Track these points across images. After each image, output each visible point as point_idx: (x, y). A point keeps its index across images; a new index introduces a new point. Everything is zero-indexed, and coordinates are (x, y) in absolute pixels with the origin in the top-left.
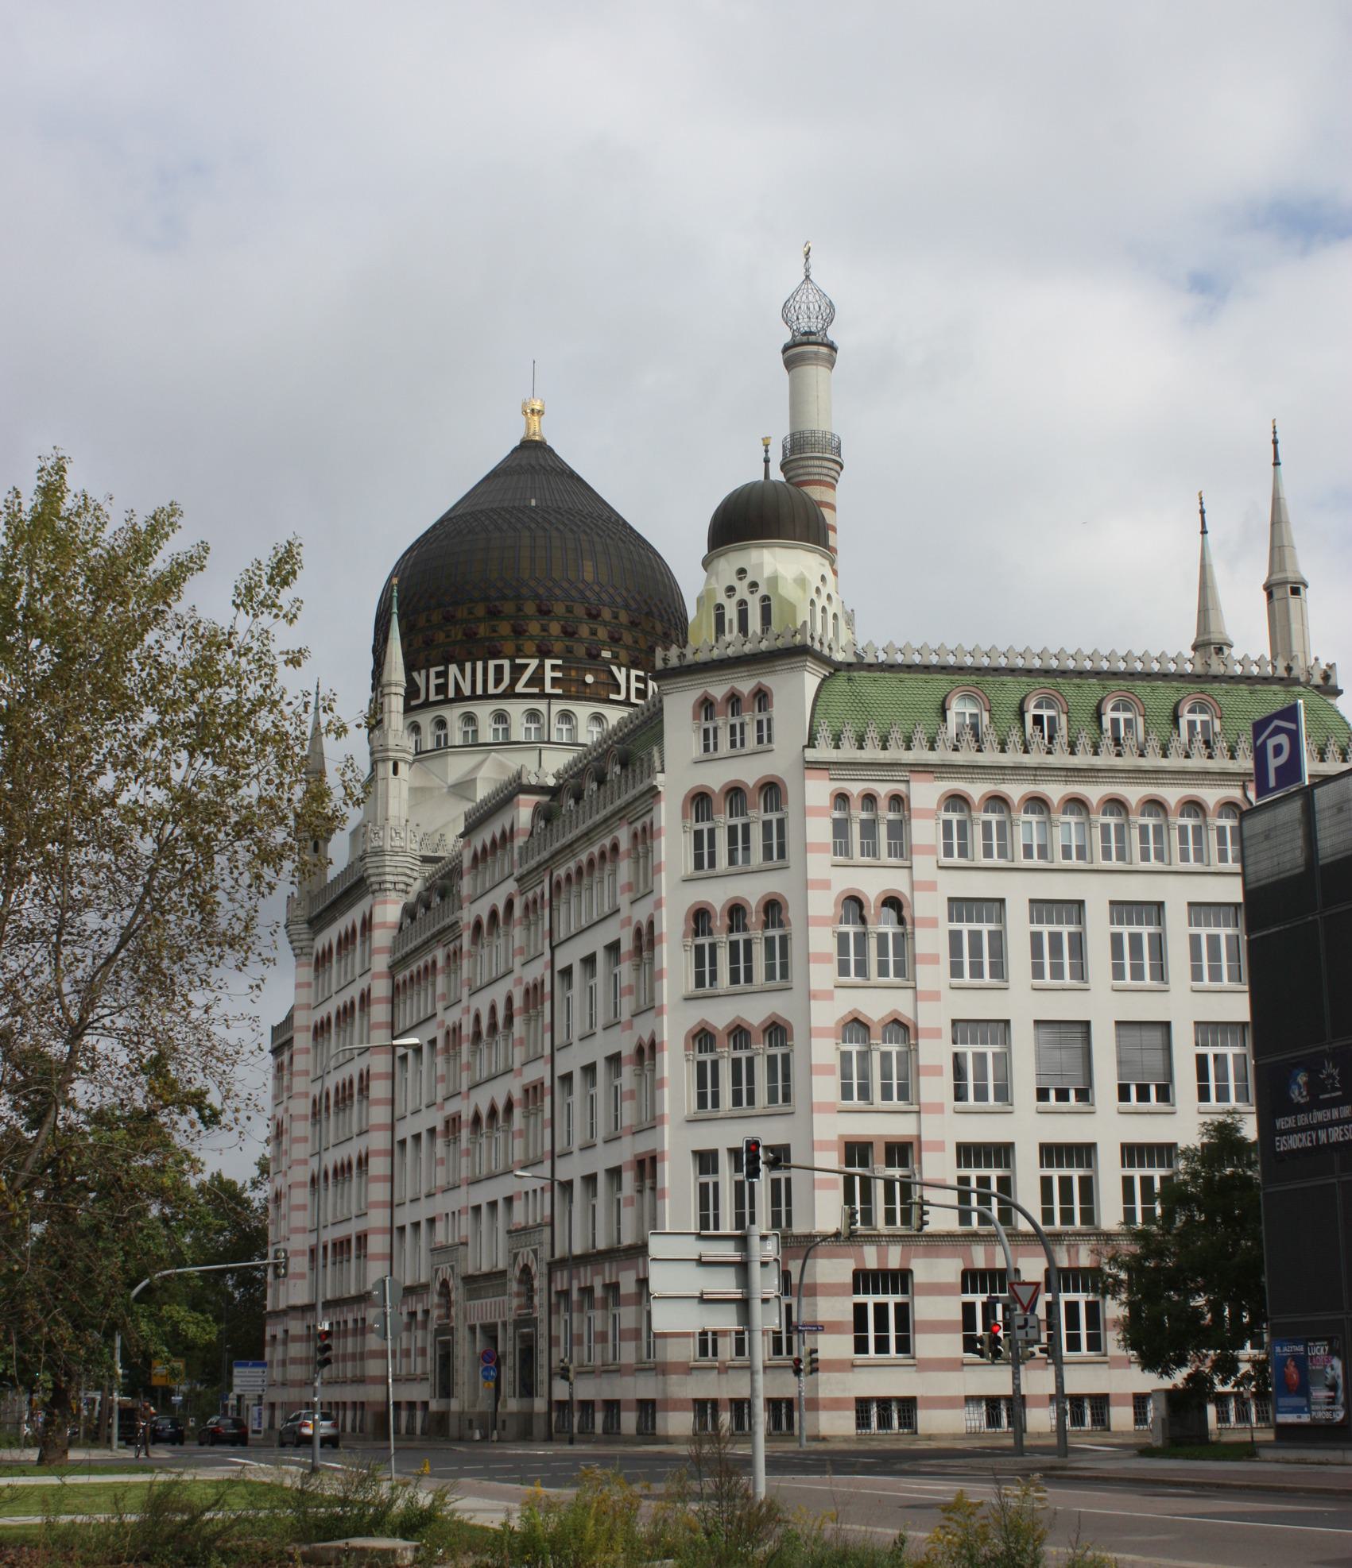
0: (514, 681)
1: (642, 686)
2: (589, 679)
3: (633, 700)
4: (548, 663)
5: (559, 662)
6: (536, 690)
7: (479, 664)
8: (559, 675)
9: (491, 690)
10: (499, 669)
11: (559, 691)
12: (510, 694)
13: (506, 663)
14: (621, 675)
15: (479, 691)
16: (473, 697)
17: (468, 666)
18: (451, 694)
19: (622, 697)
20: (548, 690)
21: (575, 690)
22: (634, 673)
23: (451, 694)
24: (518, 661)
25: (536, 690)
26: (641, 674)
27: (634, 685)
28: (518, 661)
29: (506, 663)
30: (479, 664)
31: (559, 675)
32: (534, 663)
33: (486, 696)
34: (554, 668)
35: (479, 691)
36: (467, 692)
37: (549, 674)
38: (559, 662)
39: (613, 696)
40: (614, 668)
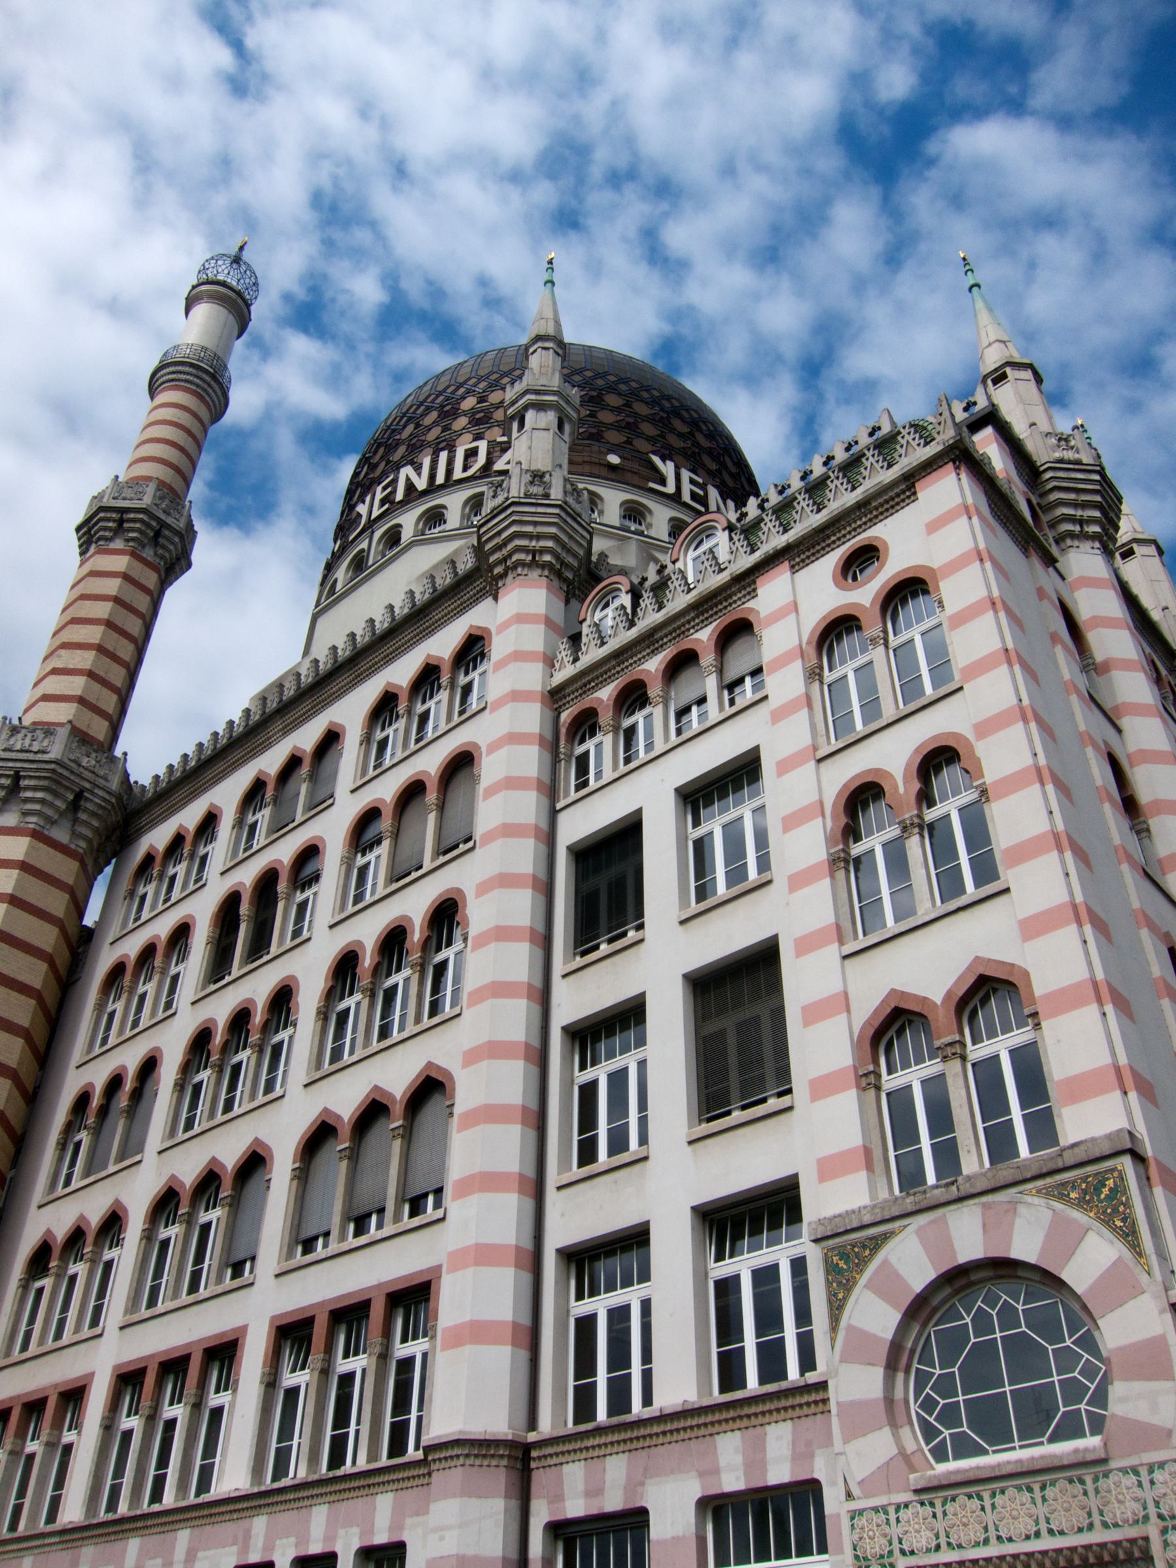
1: (701, 493)
3: (686, 497)
7: (443, 456)
9: (458, 474)
14: (668, 469)
15: (440, 479)
16: (433, 488)
17: (427, 462)
18: (399, 496)
19: (670, 489)
22: (686, 475)
23: (399, 496)
26: (701, 481)
27: (686, 488)
30: (443, 456)
33: (450, 483)
35: (440, 479)
36: (421, 484)
40: (656, 460)
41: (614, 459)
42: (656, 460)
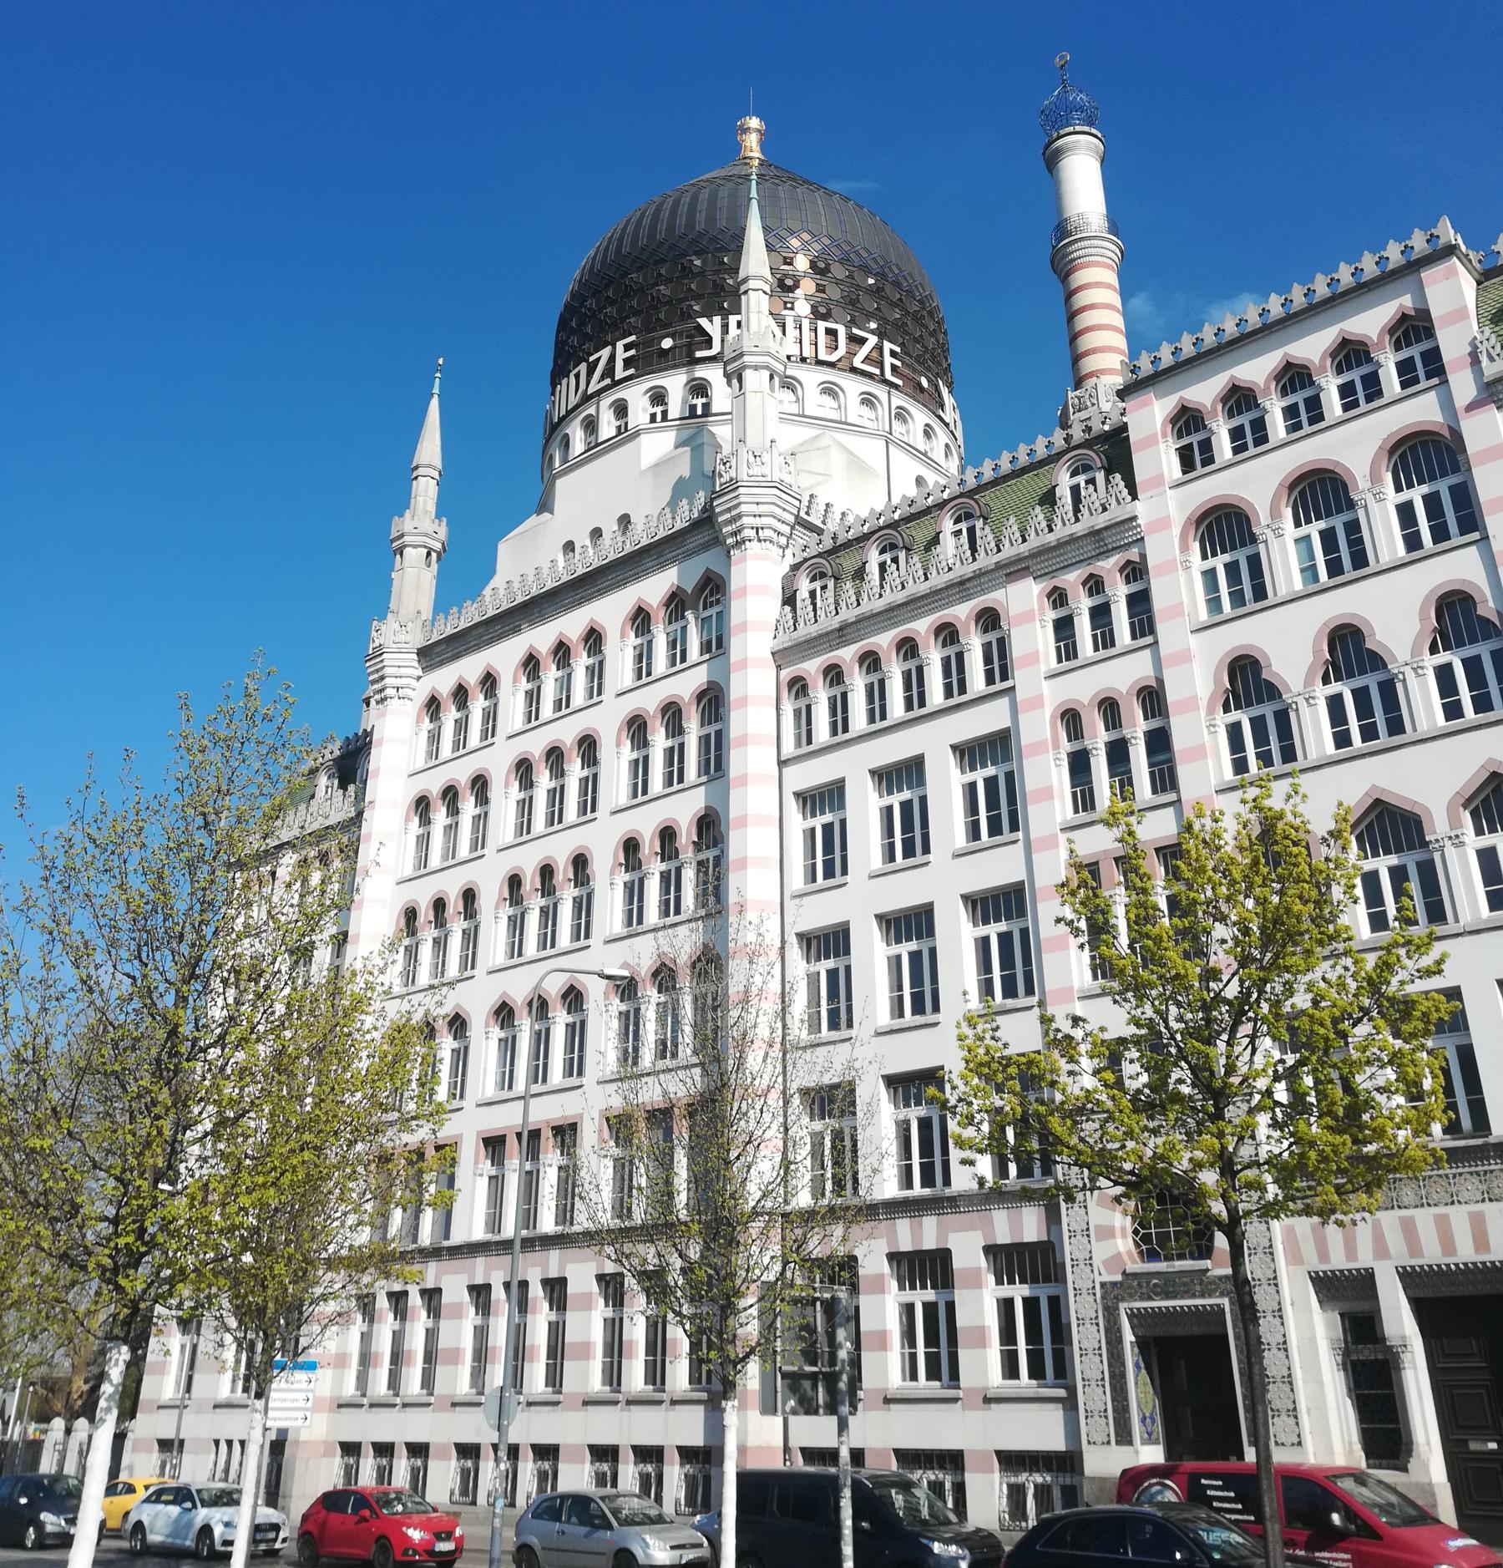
0: (588, 384)
2: (667, 343)
4: (620, 345)
5: (633, 338)
6: (608, 381)
8: (632, 352)
10: (577, 376)
11: (632, 371)
12: (587, 399)
13: (583, 367)
20: (620, 373)
21: (646, 361)
24: (591, 359)
25: (608, 381)
28: (591, 359)
29: (583, 367)
31: (632, 352)
32: (605, 353)
34: (627, 348)
37: (621, 355)
38: (633, 338)
39: (699, 354)
40: (703, 322)
41: (667, 343)
42: (703, 322)
